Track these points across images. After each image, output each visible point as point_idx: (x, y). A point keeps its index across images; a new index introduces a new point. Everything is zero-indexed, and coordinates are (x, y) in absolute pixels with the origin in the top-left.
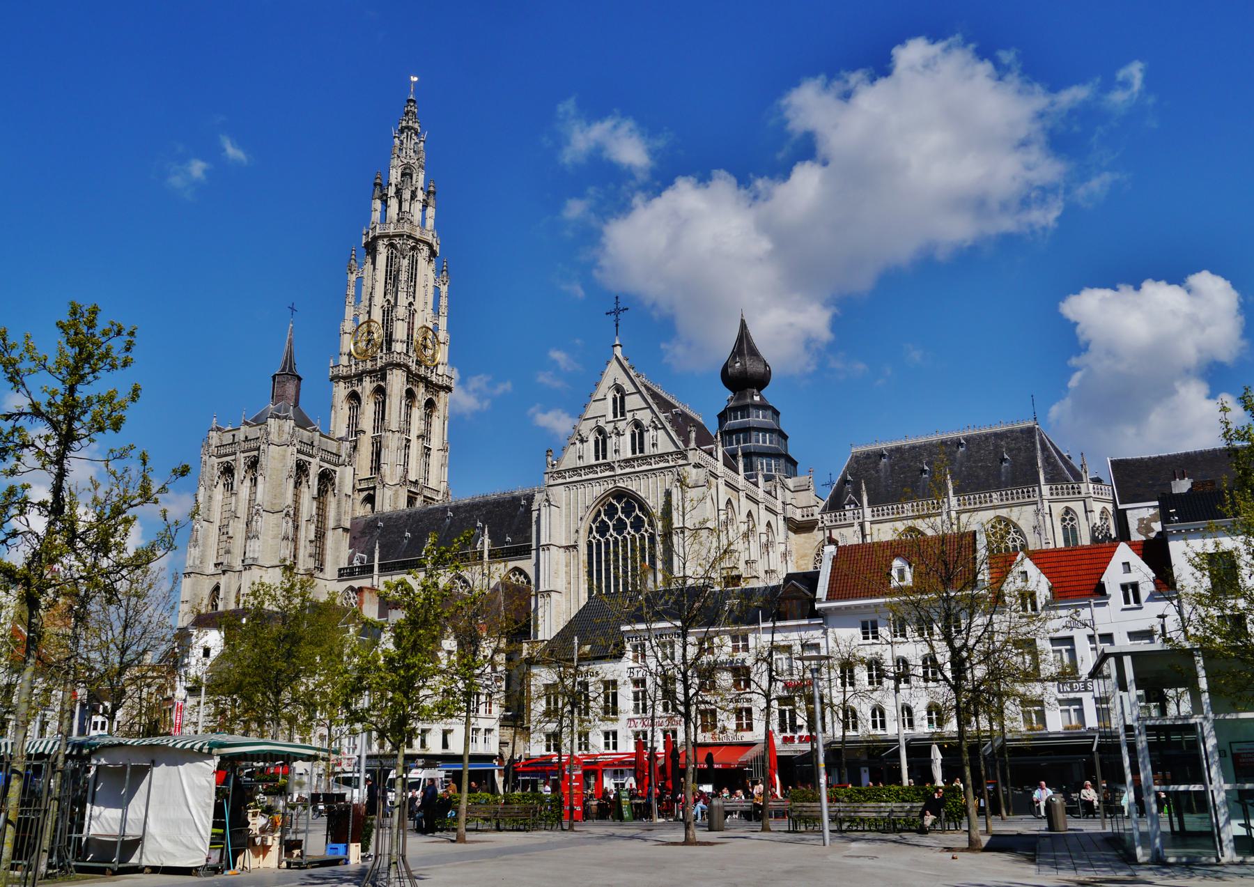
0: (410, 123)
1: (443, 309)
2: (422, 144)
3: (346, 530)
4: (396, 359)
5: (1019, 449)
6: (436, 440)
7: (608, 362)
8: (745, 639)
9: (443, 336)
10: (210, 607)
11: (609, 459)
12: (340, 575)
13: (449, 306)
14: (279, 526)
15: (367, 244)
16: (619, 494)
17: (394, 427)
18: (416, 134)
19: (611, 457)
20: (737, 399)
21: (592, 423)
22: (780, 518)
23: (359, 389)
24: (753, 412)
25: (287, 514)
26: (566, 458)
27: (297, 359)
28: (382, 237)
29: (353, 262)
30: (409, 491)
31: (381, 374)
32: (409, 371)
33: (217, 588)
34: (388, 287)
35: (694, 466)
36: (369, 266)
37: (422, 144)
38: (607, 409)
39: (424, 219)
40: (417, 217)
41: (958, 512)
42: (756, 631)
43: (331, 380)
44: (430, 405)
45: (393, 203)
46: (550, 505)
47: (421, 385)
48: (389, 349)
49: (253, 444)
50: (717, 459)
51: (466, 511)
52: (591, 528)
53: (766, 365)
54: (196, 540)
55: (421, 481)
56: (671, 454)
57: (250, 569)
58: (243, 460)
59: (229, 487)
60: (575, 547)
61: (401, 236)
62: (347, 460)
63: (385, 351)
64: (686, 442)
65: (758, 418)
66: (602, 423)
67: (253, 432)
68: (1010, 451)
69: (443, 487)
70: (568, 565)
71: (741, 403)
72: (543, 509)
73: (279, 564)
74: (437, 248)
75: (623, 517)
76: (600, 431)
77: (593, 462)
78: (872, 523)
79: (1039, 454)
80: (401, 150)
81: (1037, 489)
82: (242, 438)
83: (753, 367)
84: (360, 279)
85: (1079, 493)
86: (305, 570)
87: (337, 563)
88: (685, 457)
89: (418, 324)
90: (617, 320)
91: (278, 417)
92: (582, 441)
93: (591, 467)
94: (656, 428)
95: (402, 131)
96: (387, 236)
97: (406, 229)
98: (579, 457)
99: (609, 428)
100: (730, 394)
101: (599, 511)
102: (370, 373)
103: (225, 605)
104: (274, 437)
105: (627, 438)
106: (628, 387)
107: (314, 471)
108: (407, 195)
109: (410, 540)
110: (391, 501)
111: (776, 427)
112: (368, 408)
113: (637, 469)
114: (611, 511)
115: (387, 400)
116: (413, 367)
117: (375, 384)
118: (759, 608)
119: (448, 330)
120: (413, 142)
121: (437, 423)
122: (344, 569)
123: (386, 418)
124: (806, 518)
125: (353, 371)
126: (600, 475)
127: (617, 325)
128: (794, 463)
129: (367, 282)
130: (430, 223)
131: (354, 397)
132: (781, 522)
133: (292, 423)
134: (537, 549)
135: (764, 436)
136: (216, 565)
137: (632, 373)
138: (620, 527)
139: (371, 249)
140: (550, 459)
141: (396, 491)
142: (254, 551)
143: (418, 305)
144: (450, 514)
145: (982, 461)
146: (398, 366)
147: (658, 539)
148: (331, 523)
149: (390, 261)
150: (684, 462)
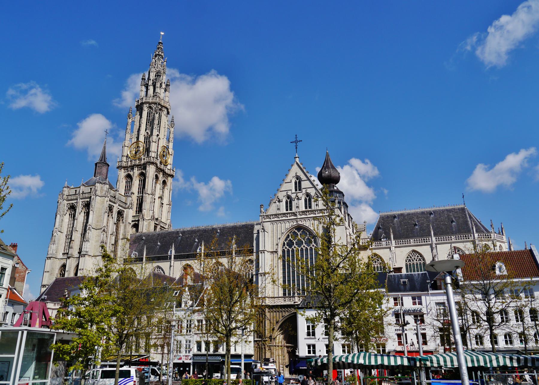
0: (160, 53)
1: (171, 139)
2: (165, 62)
4: (152, 160)
5: (459, 217)
6: (166, 200)
7: (292, 165)
8: (420, 298)
9: (171, 151)
10: (59, 275)
11: (294, 210)
14: (99, 236)
16: (299, 228)
17: (149, 192)
18: (162, 58)
19: (294, 210)
21: (285, 193)
23: (131, 173)
25: (104, 231)
26: (271, 209)
28: (146, 103)
29: (130, 113)
30: (155, 223)
31: (144, 167)
32: (157, 167)
33: (64, 266)
34: (148, 126)
36: (138, 117)
37: (165, 62)
38: (292, 187)
41: (436, 244)
42: (428, 295)
43: (118, 168)
44: (164, 183)
45: (151, 88)
46: (264, 231)
47: (161, 173)
48: (148, 155)
49: (87, 195)
51: (188, 234)
54: (54, 241)
55: (159, 219)
57: (84, 256)
58: (81, 203)
60: (276, 252)
61: (155, 103)
63: (146, 156)
66: (289, 193)
67: (87, 190)
68: (455, 218)
69: (168, 222)
72: (261, 233)
76: (289, 197)
77: (285, 211)
78: (395, 247)
79: (469, 219)
80: (155, 64)
81: (430, 238)
82: (81, 192)
83: (334, 174)
84: (133, 122)
85: (491, 238)
89: (161, 145)
92: (279, 201)
93: (284, 214)
95: (156, 56)
97: (158, 100)
98: (278, 209)
99: (293, 196)
104: (98, 193)
105: (302, 202)
106: (303, 177)
108: (158, 85)
109: (161, 247)
110: (146, 227)
112: (136, 182)
113: (308, 216)
115: (147, 179)
116: (159, 165)
117: (140, 171)
119: (173, 149)
120: (161, 61)
123: (146, 187)
126: (289, 218)
127: (296, 148)
131: (129, 177)
136: (64, 254)
137: (305, 171)
140: (262, 209)
141: (149, 222)
142: (87, 248)
144: (181, 235)
145: (442, 221)
146: (153, 163)
148: (121, 236)
149: (149, 114)
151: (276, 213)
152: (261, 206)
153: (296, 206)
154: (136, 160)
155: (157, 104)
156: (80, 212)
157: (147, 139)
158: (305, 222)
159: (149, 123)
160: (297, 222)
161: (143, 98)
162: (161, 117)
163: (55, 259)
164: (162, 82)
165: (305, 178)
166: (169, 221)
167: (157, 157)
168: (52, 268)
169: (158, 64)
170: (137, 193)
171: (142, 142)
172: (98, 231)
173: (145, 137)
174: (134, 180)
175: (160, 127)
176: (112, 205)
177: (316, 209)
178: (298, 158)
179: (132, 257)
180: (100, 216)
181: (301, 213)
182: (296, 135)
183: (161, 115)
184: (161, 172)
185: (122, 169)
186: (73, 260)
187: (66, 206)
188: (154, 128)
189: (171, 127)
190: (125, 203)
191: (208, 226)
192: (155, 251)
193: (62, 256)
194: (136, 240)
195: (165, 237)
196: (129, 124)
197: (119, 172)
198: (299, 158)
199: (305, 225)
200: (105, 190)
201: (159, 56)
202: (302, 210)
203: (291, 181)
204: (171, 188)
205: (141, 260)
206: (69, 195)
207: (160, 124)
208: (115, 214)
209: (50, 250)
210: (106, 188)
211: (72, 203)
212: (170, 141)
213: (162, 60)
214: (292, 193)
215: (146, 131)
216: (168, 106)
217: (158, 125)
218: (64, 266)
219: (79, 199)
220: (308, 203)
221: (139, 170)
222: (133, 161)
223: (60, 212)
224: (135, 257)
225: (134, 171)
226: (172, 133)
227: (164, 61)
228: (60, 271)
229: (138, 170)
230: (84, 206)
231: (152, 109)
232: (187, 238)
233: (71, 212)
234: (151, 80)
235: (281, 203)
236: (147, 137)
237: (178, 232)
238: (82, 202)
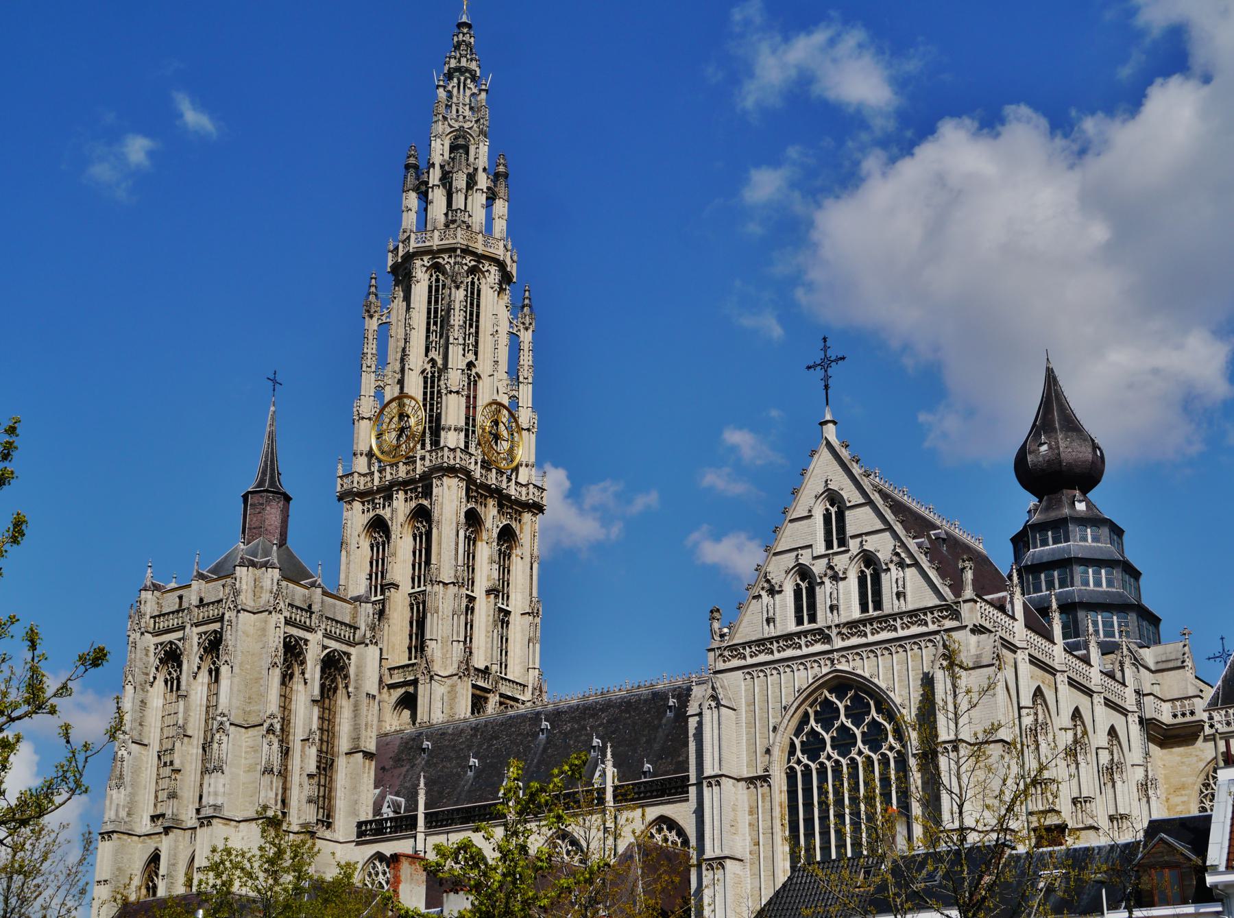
0: (464, 63)
1: (526, 372)
2: (483, 95)
3: (368, 755)
4: (448, 459)
6: (519, 596)
9: (525, 416)
10: (144, 891)
11: (821, 623)
12: (360, 834)
13: (535, 366)
14: (256, 749)
15: (395, 269)
16: (842, 684)
17: (447, 575)
18: (474, 79)
19: (824, 618)
20: (1047, 509)
21: (789, 561)
22: (1133, 719)
23: (386, 513)
24: (1075, 530)
25: (270, 730)
26: (744, 623)
27: (282, 465)
28: (419, 253)
29: (372, 298)
30: (474, 686)
31: (422, 486)
33: (155, 858)
34: (433, 337)
35: (973, 631)
36: (399, 304)
37: (483, 95)
38: (814, 534)
39: (490, 219)
40: (478, 216)
43: (340, 499)
44: (507, 536)
46: (718, 705)
47: (491, 503)
48: (436, 443)
49: (212, 612)
50: (1013, 618)
51: (573, 719)
52: (792, 745)
53: (1095, 447)
54: (121, 777)
55: (495, 668)
56: (931, 610)
57: (209, 824)
59: (174, 684)
60: (765, 778)
61: (451, 250)
62: (368, 635)
63: (428, 447)
64: (957, 588)
65: (1084, 542)
66: (805, 559)
67: (212, 591)
69: (532, 678)
70: (753, 811)
71: (1053, 515)
73: (256, 816)
74: (513, 269)
75: (849, 724)
76: (804, 572)
77: (792, 627)
80: (448, 107)
82: (195, 602)
84: (385, 326)
86: (302, 825)
87: (355, 813)
88: (956, 615)
89: (484, 397)
90: (826, 378)
91: (253, 564)
92: (772, 592)
93: (788, 637)
94: (902, 565)
95: (449, 76)
96: (429, 252)
98: (768, 621)
99: (819, 568)
100: (1032, 501)
101: (806, 714)
102: (404, 485)
103: (170, 886)
104: (246, 599)
106: (850, 494)
107: (313, 655)
108: (460, 181)
109: (479, 772)
111: (1117, 556)
112: (403, 544)
113: (871, 639)
114: (827, 714)
115: (434, 531)
116: (477, 472)
117: (413, 504)
118: (1101, 883)
119: (535, 407)
120: (468, 93)
121: (519, 568)
122: (366, 823)
123: (433, 561)
124: (1180, 720)
125: (376, 482)
126: (805, 651)
127: (826, 387)
128: (1155, 621)
129: (397, 331)
130: (500, 226)
131: (379, 526)
132: (1135, 729)
133: (276, 574)
134: (699, 784)
135: (1098, 573)
136: (154, 818)
137: (856, 470)
138: (844, 742)
139: (402, 274)
140: (716, 625)
141: (453, 686)
142: (216, 794)
143: (483, 367)
144: (545, 724)
146: (452, 471)
147: (912, 762)
148: (343, 744)
149: (434, 293)
150: (955, 624)
151: (760, 636)
152: (712, 612)
153: (895, 590)
154: (396, 464)
155: (459, 252)
156: (196, 670)
157: (432, 382)
158: (858, 662)
159: (436, 323)
160: (832, 661)
161: (409, 238)
162: (479, 295)
163: (125, 837)
164: (476, 170)
165: (857, 498)
166: (534, 674)
167: (467, 446)
168: (119, 869)
169: (457, 105)
170: (410, 584)
171: (412, 398)
172: (251, 732)
173: (425, 378)
174: (393, 536)
175: (477, 332)
176: (301, 639)
177: (896, 610)
178: (831, 425)
179: (385, 816)
180: (257, 680)
181: (844, 631)
182: (825, 339)
183: (479, 291)
184: (492, 496)
185: (353, 500)
186: (181, 839)
187: (151, 654)
188: (451, 340)
189: (521, 327)
190: (351, 626)
191: (639, 687)
192: (459, 790)
193: (148, 827)
194: (402, 752)
195: (497, 738)
196: (370, 337)
197: (345, 513)
198: (835, 423)
199: (859, 672)
200: (269, 587)
201: (462, 73)
202: (849, 619)
203: (810, 511)
204: (536, 553)
205: (411, 823)
207: (477, 321)
208: (313, 670)
209: (110, 810)
210: (269, 582)
211: (171, 643)
212: (521, 379)
213: (472, 86)
214: (815, 558)
215: (426, 355)
217: (471, 326)
218: (155, 858)
219: (188, 626)
220: (871, 591)
221: (411, 500)
222: (388, 468)
223: (133, 676)
224: (391, 815)
225: (395, 503)
226: (526, 349)
227: (481, 90)
228: (146, 876)
229: (406, 501)
230: (205, 649)
231: (444, 273)
232: (566, 735)
233: (170, 673)
234: (437, 167)
235: (777, 596)
236: (433, 376)
237: (538, 714)
238: (200, 634)
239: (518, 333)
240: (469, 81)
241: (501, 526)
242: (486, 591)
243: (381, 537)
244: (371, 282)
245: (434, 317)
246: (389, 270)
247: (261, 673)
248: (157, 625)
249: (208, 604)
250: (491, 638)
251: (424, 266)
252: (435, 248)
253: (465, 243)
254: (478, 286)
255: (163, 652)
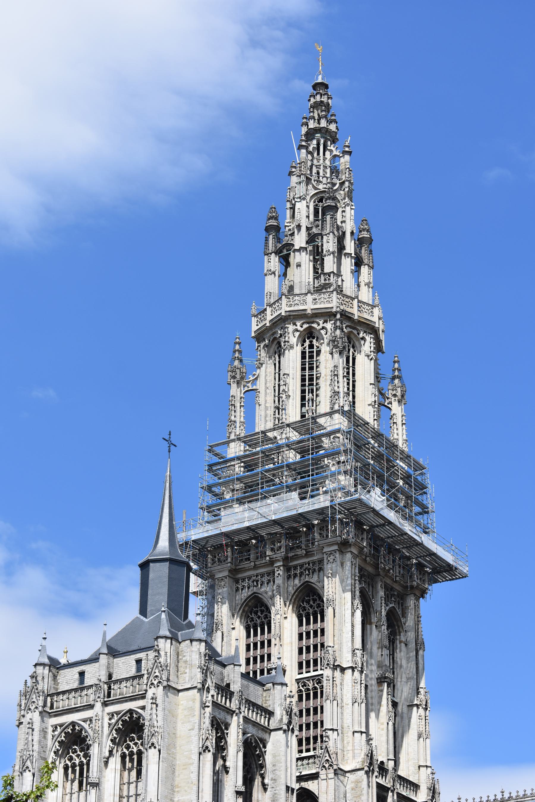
15: (259, 337)
29: (236, 363)
61: (328, 315)
155: (338, 316)
156: (107, 754)
187: (50, 737)
196: (238, 405)
206: (58, 694)
207: (354, 391)
211: (73, 724)
216: (375, 319)
226: (399, 423)
239: (390, 406)
240: (329, 143)
241: (388, 608)
242: (377, 679)
243: (259, 617)
244: (235, 347)
245: (309, 385)
246: (253, 335)
247: (190, 758)
248: (55, 704)
249: (120, 681)
250: (385, 731)
251: (297, 330)
252: (309, 311)
253: (342, 307)
254: (353, 354)
255: (63, 735)
